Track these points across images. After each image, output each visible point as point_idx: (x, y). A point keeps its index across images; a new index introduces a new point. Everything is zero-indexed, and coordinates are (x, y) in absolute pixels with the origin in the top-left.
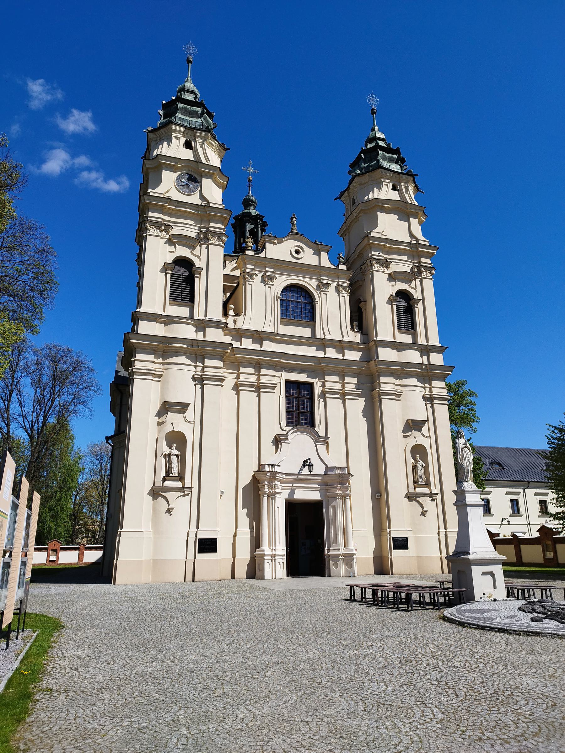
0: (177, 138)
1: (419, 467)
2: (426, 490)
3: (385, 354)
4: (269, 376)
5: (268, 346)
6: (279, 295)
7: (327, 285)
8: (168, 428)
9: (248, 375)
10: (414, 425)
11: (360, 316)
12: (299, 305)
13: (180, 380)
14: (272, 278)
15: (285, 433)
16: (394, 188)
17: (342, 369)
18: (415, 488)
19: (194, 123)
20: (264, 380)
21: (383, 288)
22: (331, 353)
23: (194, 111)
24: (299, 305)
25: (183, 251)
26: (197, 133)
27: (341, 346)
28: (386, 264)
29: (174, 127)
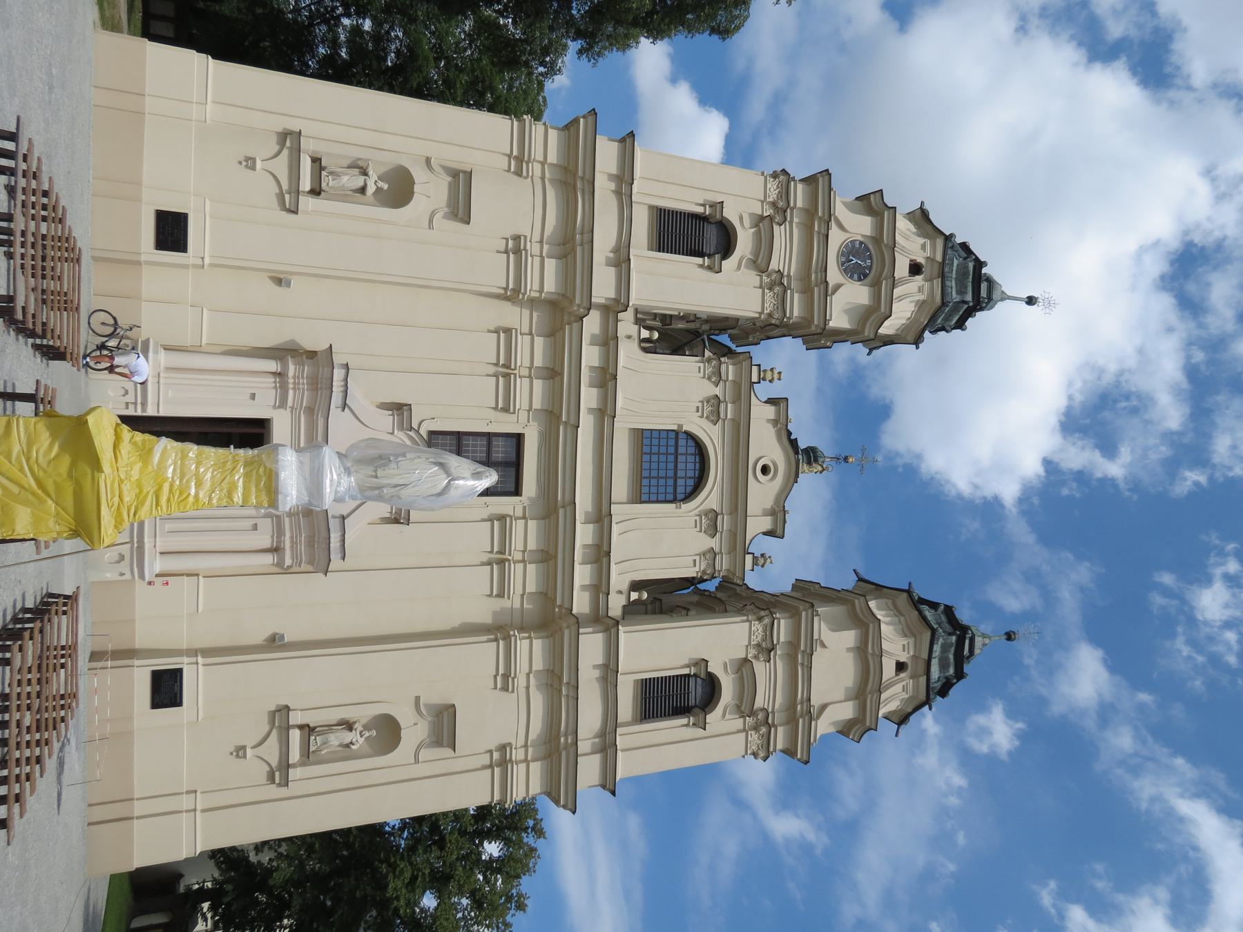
1: (348, 737)
2: (295, 755)
3: (591, 646)
4: (530, 394)
5: (589, 397)
7: (713, 530)
8: (419, 174)
9: (531, 351)
10: (444, 725)
11: (663, 599)
13: (516, 207)
14: (715, 417)
15: (415, 426)
17: (552, 557)
18: (301, 727)
20: (521, 387)
22: (584, 534)
23: (966, 287)
26: (937, 283)
28: (766, 650)
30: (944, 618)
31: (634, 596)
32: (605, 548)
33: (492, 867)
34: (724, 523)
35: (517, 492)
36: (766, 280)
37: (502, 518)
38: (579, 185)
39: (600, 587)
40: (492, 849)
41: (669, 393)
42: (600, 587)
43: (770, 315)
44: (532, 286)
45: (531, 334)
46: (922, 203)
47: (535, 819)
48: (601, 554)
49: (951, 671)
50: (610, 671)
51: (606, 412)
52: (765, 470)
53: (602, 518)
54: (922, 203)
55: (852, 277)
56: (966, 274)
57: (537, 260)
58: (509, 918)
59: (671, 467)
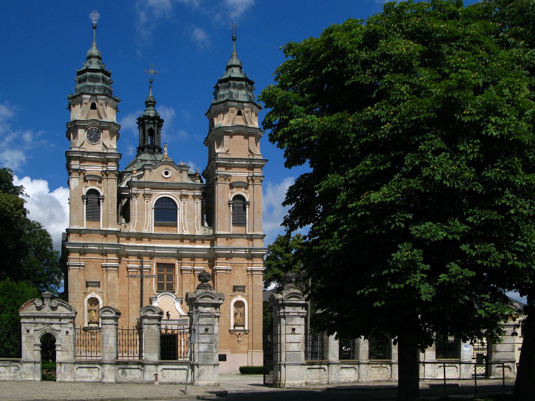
0: (86, 104)
6: (153, 207)
11: (209, 214)
12: (166, 212)
14: (150, 196)
16: (239, 113)
21: (224, 195)
24: (166, 212)
27: (193, 239)
29: (84, 96)
30: (223, 84)
31: (206, 224)
34: (184, 192)
35: (173, 265)
36: (105, 176)
37: (181, 270)
39: (202, 239)
42: (202, 239)
43: (116, 175)
50: (228, 237)
51: (150, 237)
52: (167, 173)
53: (182, 238)
56: (92, 76)
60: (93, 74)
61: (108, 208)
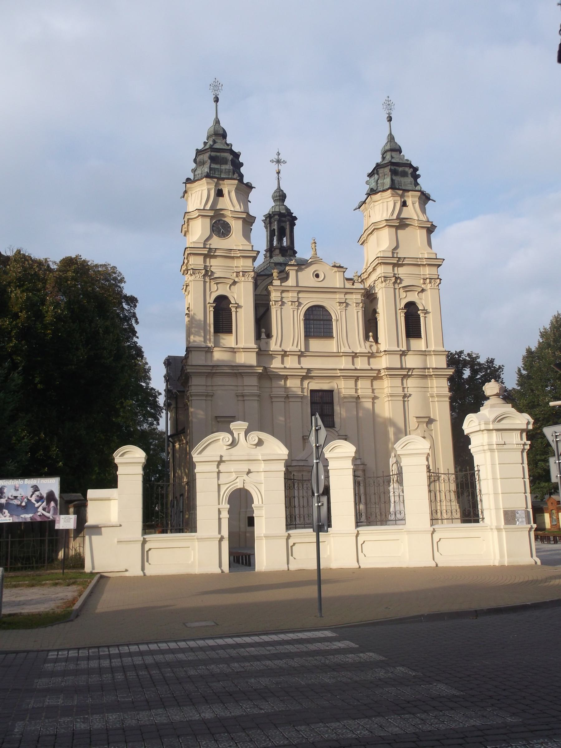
19: (224, 171)
23: (223, 158)
25: (223, 290)
26: (226, 182)
31: (371, 339)
32: (354, 354)
33: (474, 372)
38: (214, 371)
40: (467, 373)
41: (287, 324)
44: (255, 391)
45: (271, 388)
46: (184, 183)
47: (455, 354)
48: (355, 356)
49: (407, 169)
52: (317, 276)
54: (184, 183)
55: (230, 232)
57: (245, 388)
58: (497, 367)
59: (318, 323)
60: (218, 154)
61: (244, 319)
